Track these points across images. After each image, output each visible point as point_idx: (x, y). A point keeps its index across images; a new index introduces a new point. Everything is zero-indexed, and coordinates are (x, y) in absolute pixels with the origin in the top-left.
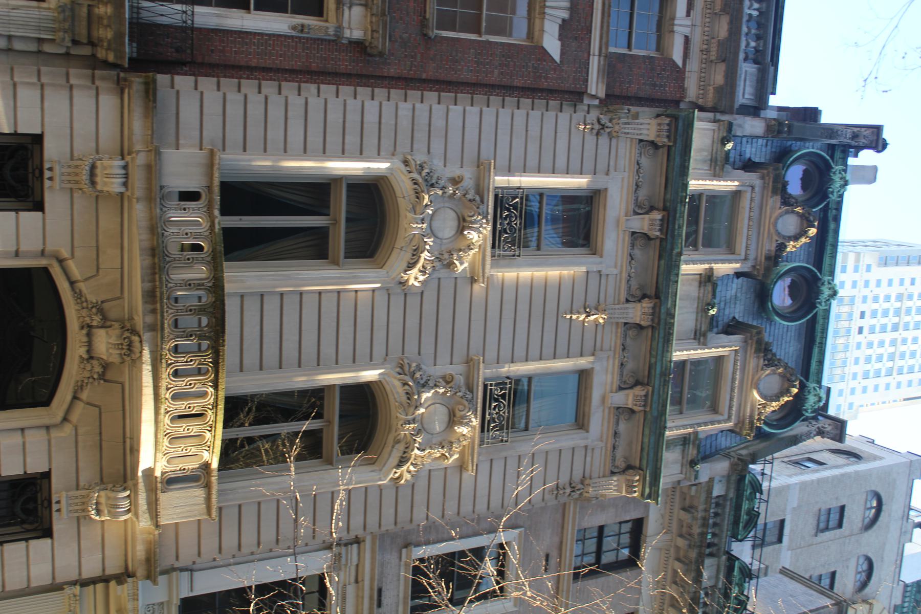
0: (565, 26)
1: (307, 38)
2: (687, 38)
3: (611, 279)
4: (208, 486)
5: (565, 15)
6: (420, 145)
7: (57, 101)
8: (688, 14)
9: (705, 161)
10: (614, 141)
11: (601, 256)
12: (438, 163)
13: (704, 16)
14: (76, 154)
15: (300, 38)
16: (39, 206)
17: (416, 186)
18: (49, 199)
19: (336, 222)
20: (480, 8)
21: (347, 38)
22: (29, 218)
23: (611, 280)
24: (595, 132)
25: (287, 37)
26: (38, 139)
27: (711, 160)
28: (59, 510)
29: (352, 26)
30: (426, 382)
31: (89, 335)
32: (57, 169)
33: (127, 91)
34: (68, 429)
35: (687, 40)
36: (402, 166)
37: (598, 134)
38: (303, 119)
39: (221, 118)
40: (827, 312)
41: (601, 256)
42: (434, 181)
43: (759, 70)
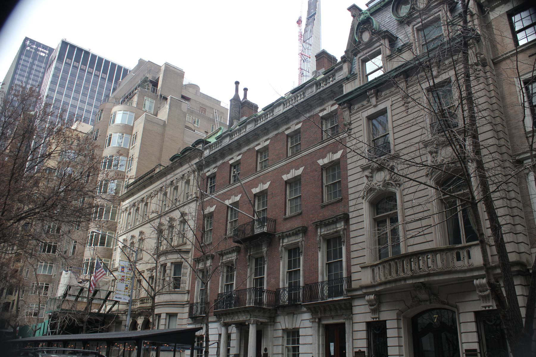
0: (335, 152)
2: (331, 106)
3: (393, 99)
4: (470, 246)
5: (331, 153)
7: (357, 318)
8: (325, 109)
11: (386, 108)
16: (385, 321)
19: (388, 215)
20: (336, 182)
22: (389, 325)
23: (393, 99)
24: (350, 131)
25: (347, 246)
26: (368, 324)
30: (433, 162)
31: (421, 302)
32: (373, 316)
34: (458, 304)
41: (386, 108)
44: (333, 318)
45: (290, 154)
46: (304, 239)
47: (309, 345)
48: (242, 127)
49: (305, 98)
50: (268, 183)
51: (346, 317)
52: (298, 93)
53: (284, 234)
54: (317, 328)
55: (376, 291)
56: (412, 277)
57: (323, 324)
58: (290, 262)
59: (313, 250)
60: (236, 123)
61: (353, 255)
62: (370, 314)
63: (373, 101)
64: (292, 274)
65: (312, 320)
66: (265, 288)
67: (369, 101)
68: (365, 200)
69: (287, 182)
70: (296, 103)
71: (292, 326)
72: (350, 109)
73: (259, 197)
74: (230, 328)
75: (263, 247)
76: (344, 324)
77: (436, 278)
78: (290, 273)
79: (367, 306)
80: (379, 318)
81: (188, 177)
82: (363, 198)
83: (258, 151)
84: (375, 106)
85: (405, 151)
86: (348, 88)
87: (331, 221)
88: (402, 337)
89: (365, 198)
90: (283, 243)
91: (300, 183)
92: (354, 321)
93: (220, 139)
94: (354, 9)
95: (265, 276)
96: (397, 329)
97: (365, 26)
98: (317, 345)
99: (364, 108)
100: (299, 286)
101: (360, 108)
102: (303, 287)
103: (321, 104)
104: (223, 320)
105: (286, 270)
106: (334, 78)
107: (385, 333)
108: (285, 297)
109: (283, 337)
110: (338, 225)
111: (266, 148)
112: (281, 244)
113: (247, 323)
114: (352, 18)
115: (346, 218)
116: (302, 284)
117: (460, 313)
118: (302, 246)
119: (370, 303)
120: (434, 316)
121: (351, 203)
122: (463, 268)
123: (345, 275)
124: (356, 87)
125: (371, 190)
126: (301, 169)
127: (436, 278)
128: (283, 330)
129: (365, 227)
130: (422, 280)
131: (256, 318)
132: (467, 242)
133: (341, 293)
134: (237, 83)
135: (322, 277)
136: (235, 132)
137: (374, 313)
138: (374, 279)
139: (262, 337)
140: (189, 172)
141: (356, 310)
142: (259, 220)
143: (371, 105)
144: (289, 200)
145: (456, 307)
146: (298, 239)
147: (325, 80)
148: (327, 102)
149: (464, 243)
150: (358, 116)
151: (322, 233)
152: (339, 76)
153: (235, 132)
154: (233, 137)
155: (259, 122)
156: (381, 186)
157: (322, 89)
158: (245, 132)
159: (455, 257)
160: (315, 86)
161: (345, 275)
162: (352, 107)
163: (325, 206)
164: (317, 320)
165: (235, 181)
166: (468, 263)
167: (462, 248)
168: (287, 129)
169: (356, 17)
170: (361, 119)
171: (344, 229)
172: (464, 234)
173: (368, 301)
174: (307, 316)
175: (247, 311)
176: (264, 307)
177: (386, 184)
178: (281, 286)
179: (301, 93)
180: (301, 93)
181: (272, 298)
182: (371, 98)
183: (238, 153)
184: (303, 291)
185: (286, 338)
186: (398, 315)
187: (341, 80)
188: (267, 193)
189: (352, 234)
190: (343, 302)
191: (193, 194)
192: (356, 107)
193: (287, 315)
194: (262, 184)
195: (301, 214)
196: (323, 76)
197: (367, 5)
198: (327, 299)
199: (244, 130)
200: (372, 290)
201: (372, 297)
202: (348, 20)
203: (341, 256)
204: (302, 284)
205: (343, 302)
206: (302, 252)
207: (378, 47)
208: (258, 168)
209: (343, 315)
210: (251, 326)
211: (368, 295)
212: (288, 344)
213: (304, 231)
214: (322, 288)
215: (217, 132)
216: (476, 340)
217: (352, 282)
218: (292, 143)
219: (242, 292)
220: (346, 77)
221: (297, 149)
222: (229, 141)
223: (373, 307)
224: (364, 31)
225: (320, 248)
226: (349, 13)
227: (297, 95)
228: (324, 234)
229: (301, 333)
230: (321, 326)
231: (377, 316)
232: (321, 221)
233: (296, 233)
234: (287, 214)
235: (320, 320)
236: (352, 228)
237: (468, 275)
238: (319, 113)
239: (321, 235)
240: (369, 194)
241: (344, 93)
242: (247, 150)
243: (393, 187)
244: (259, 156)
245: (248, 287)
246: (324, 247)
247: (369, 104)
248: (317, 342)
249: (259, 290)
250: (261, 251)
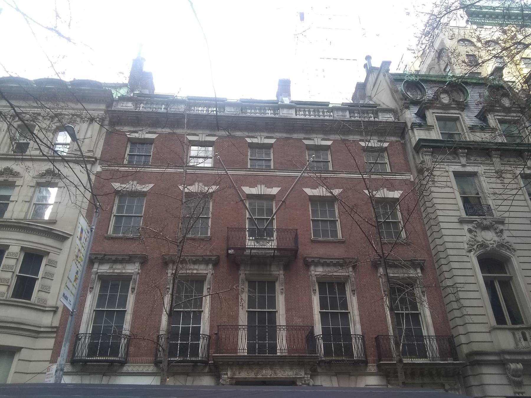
0: (390, 190)
5: (385, 189)
6: (461, 245)
9: (429, 133)
12: (465, 239)
14: (508, 383)
17: (479, 247)
27: (428, 130)
32: (517, 390)
33: (479, 362)
37: (434, 176)
43: (380, 112)
52: (321, 109)
59: (372, 292)
68: (474, 254)
82: (470, 251)
84: (464, 166)
85: (511, 221)
138: (517, 345)
143: (460, 163)
146: (349, 272)
156: (495, 245)
168: (305, 139)
173: (514, 370)
177: (501, 245)
193: (336, 375)
201: (520, 366)
207: (455, 114)
224: (446, 93)
233: (341, 263)
240: (478, 249)
243: (507, 250)
250: (268, 273)
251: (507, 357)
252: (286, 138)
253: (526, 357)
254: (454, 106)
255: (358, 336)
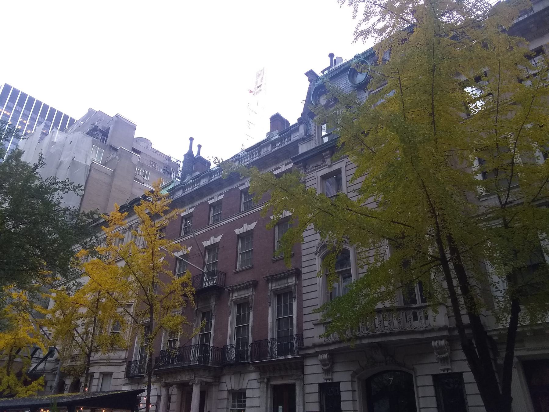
1: (297, 295)
7: (309, 379)
8: (280, 168)
10: (306, 181)
12: (317, 242)
13: (280, 162)
14: (322, 372)
15: (298, 297)
16: (338, 383)
18: (336, 380)
21: (296, 281)
22: (343, 387)
26: (321, 385)
27: (310, 141)
28: (448, 370)
29: (292, 281)
32: (326, 377)
34: (415, 366)
35: (287, 164)
36: (318, 255)
38: (309, 293)
39: (310, 322)
40: (363, 54)
42: (321, 242)
43: (292, 133)
44: (282, 378)
45: (243, 209)
46: (254, 293)
47: (256, 408)
48: (196, 181)
49: (260, 157)
50: (220, 237)
51: (296, 378)
52: (254, 152)
53: (235, 288)
54: (265, 389)
55: (329, 351)
56: (368, 337)
57: (271, 385)
58: (238, 317)
60: (188, 178)
61: (305, 311)
62: (323, 374)
63: (328, 161)
64: (241, 330)
65: (260, 381)
66: (211, 345)
67: (324, 161)
68: (318, 256)
69: (239, 236)
70: (252, 161)
71: (239, 386)
72: (305, 167)
73: (209, 250)
74: (171, 389)
75: (212, 301)
76: (294, 385)
77: (393, 338)
78: (238, 329)
79: (320, 365)
80: (332, 379)
81: (136, 228)
82: (316, 254)
83: (211, 205)
84: (330, 166)
86: (303, 149)
87: (282, 275)
88: (357, 401)
89: (318, 254)
90: (232, 297)
91: (252, 237)
92: (306, 382)
93: (172, 192)
94: (311, 74)
95: (212, 332)
96: (351, 392)
97: (323, 90)
98: (264, 408)
99: (319, 168)
100: (248, 343)
101: (315, 168)
102: (252, 344)
103: (276, 162)
104: (164, 380)
105: (235, 326)
106: (289, 138)
107: (339, 396)
108: (232, 354)
109: (228, 399)
110: (290, 281)
111: (219, 203)
112: (230, 298)
113: (191, 384)
114: (308, 83)
115: (298, 273)
116: (250, 341)
117: (417, 376)
118: (252, 300)
119: (323, 363)
120: (389, 379)
121: (304, 259)
122: (420, 329)
123: (295, 332)
124: (312, 148)
125: (324, 246)
126: (254, 224)
127: (393, 338)
128: (229, 391)
129: (318, 282)
130: (378, 340)
131: (201, 377)
132: (422, 302)
133: (291, 351)
134: (192, 139)
135: (272, 334)
136: (189, 185)
137: (327, 374)
139: (206, 399)
140: (137, 223)
141: (308, 370)
142: (208, 273)
143: (326, 165)
144: (240, 254)
145: (413, 369)
146: (249, 293)
147: (280, 140)
148: (282, 161)
149: (419, 304)
150: (312, 175)
151: (273, 288)
152: (295, 137)
153: (189, 185)
154: (186, 190)
155: (213, 177)
157: (277, 148)
158: (198, 186)
159: (412, 317)
160: (270, 145)
161: (295, 332)
162: (307, 166)
163: (276, 261)
164: (265, 381)
165: (185, 233)
166: (426, 324)
167: (419, 308)
168: (241, 185)
169: (312, 82)
170: (316, 178)
171: (296, 284)
172: (419, 294)
173: (321, 361)
174: (254, 376)
175: (192, 369)
176: (209, 365)
178: (228, 343)
179: (257, 152)
180: (257, 152)
181: (219, 355)
182: (327, 158)
183: (190, 206)
184: (252, 347)
185: (231, 400)
186: (352, 376)
187: (297, 140)
188: (218, 246)
189: (304, 290)
190: (294, 361)
191: (140, 245)
192: (311, 167)
193: (233, 374)
194: (213, 237)
195: (251, 268)
196: (278, 136)
197: (323, 72)
198: (276, 358)
199: (198, 184)
200: (326, 349)
201: (325, 356)
202: (305, 84)
203: (292, 312)
204: (250, 341)
205: (294, 361)
206: (252, 307)
208: (210, 222)
209: (293, 375)
210: (194, 386)
211: (321, 354)
212: (233, 406)
213: (255, 285)
214: (272, 346)
215: (170, 184)
216: (435, 405)
217: (304, 340)
218: (245, 199)
219: (185, 348)
220: (302, 138)
221: (249, 206)
222: (182, 193)
223: (326, 368)
225: (270, 303)
226: (306, 78)
227: (252, 153)
228: (274, 289)
229: (247, 395)
230: (269, 385)
231: (330, 377)
232: (272, 276)
233: (246, 288)
234: (238, 267)
235: (269, 380)
236: (305, 283)
237: (426, 336)
238: (274, 171)
239: (272, 290)
240: (321, 251)
241: (300, 153)
242: (200, 203)
243: (346, 244)
244: (212, 210)
245: (193, 344)
246: (274, 302)
247: (324, 164)
248: (265, 405)
249: (204, 348)
251: (317, 349)
252: (230, 190)
253: (331, 348)
254: (333, 103)
255: (250, 344)
